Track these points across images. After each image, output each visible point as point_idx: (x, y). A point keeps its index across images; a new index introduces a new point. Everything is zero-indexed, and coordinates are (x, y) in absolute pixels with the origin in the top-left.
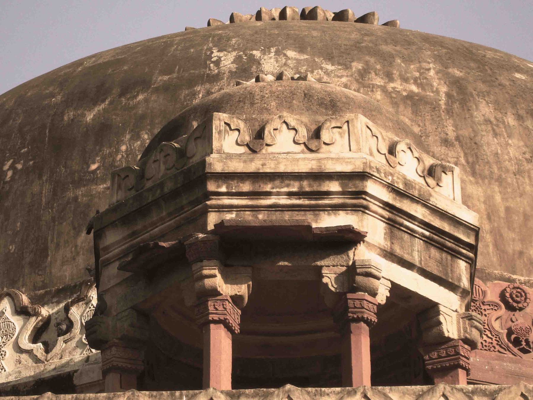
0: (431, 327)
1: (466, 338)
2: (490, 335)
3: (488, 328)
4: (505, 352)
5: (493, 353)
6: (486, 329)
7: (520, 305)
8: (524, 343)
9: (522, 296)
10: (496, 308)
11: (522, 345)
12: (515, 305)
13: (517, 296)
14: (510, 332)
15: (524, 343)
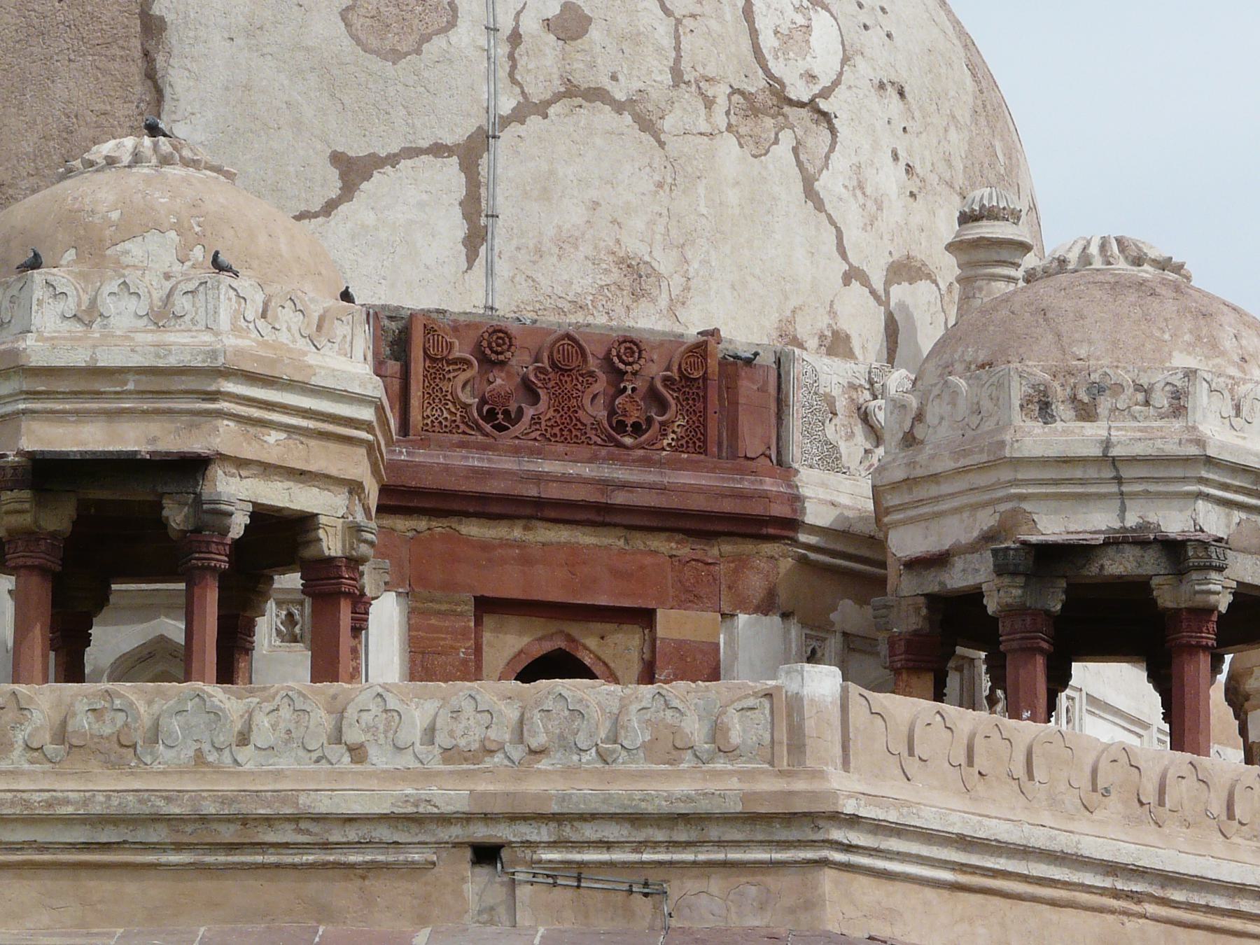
0: (308, 543)
1: (352, 555)
2: (453, 410)
3: (451, 398)
4: (473, 433)
5: (456, 435)
6: (449, 400)
7: (501, 357)
8: (500, 416)
9: (504, 343)
10: (465, 367)
11: (498, 419)
12: (493, 357)
13: (498, 345)
14: (483, 401)
15: (500, 416)
